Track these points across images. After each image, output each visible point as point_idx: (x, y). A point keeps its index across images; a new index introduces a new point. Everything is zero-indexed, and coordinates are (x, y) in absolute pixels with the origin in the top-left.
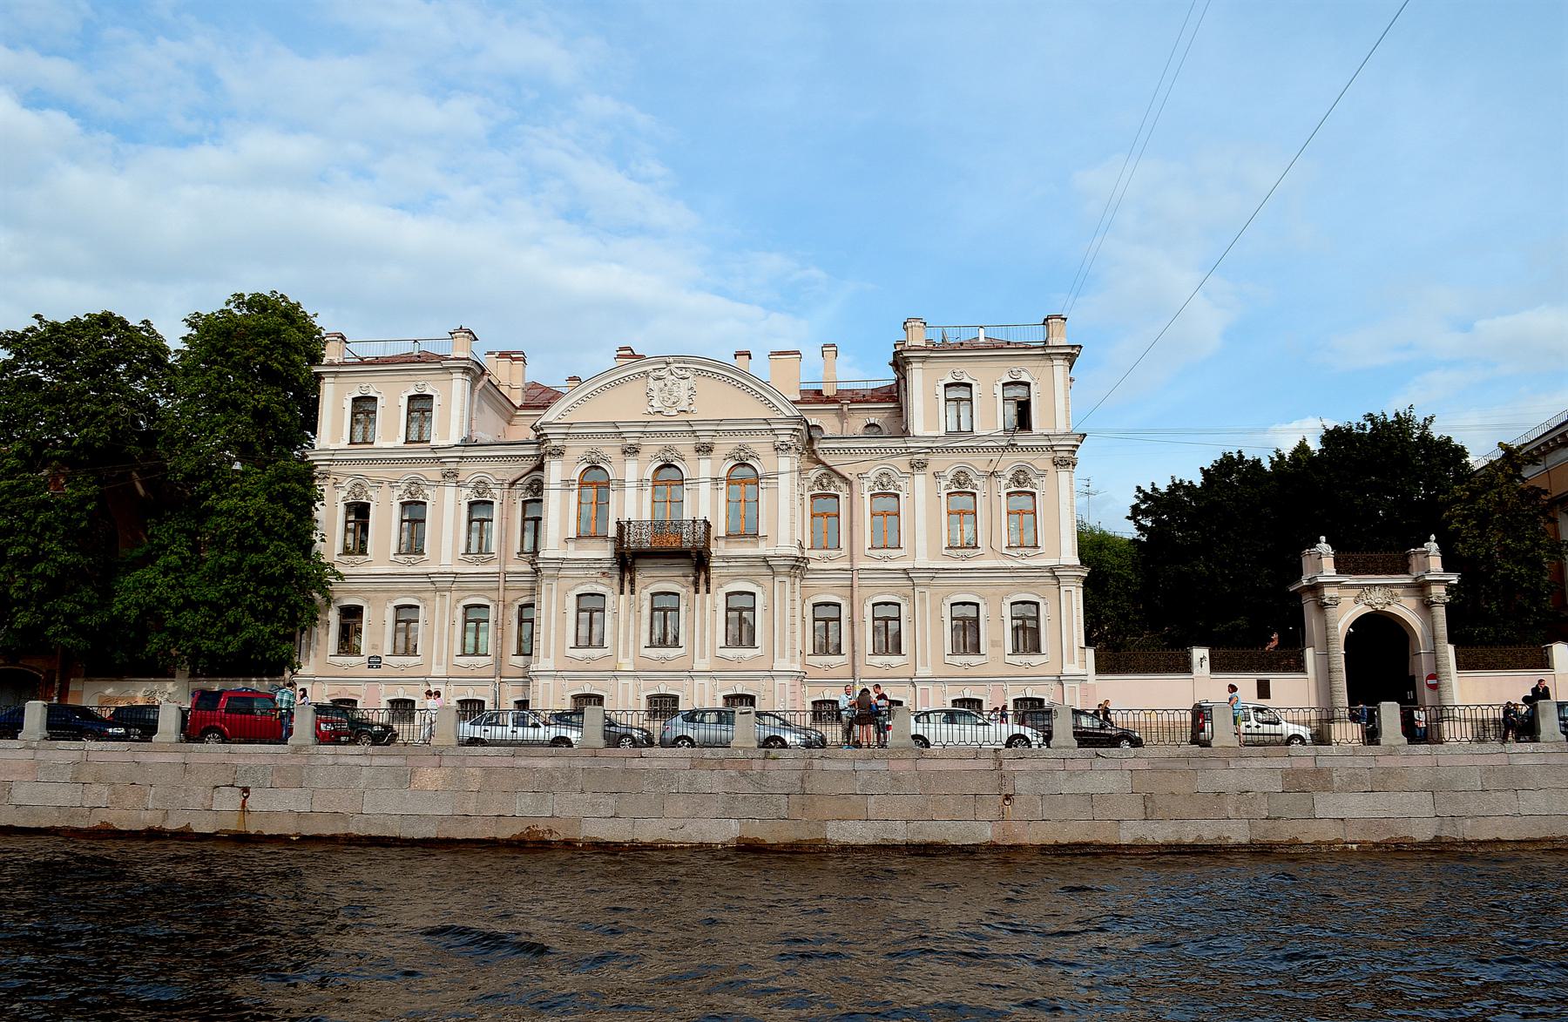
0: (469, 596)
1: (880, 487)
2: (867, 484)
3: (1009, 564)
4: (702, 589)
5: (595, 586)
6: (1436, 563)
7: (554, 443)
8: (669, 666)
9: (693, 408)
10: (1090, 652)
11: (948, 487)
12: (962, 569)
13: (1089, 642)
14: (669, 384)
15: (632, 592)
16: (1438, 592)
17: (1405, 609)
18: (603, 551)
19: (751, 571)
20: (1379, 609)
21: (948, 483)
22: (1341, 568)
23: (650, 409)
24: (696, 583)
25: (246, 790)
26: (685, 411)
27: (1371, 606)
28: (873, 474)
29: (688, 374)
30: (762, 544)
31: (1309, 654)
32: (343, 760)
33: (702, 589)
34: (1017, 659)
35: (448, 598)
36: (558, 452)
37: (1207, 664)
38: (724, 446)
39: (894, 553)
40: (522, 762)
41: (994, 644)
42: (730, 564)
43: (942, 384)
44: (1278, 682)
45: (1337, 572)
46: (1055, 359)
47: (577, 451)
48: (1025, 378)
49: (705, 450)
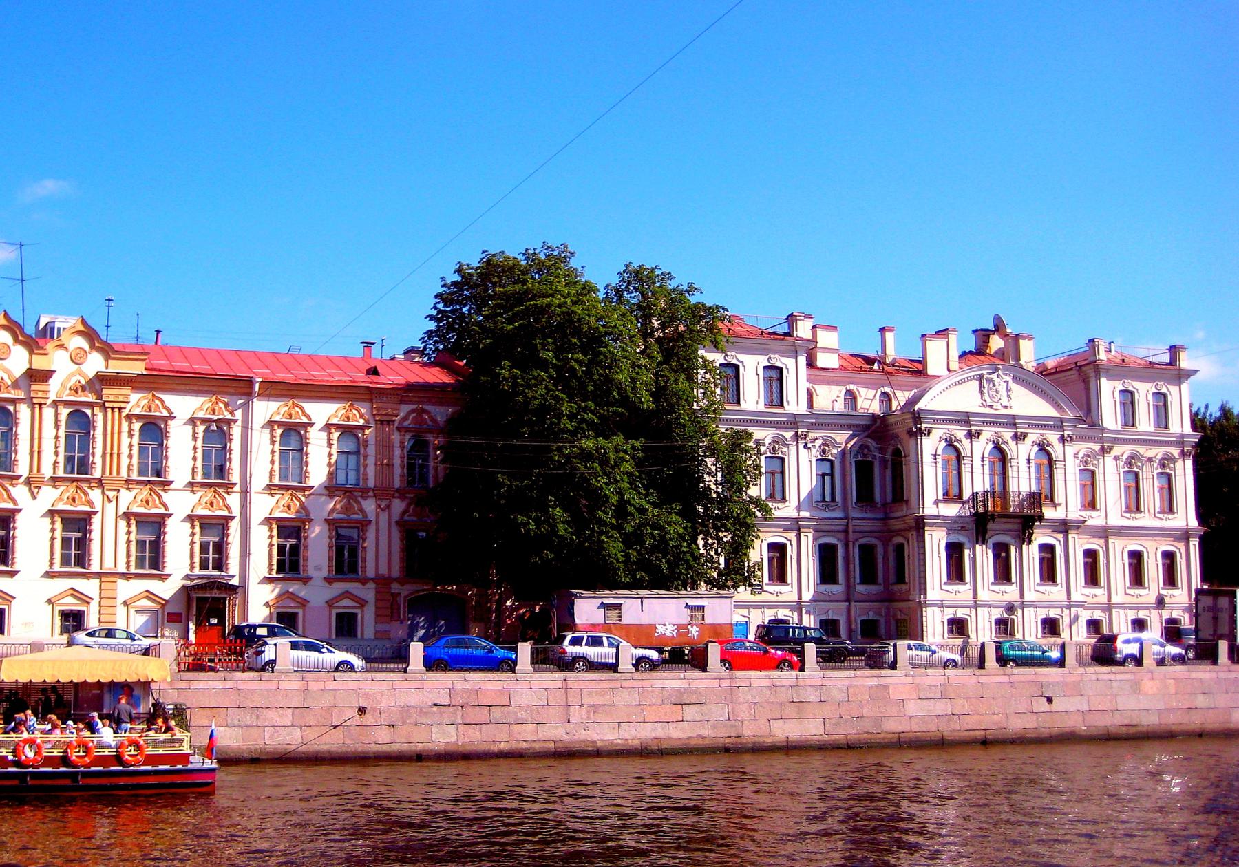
23: (984, 403)
25: (1050, 700)
32: (1100, 677)
38: (1033, 436)
40: (1194, 675)
47: (939, 432)
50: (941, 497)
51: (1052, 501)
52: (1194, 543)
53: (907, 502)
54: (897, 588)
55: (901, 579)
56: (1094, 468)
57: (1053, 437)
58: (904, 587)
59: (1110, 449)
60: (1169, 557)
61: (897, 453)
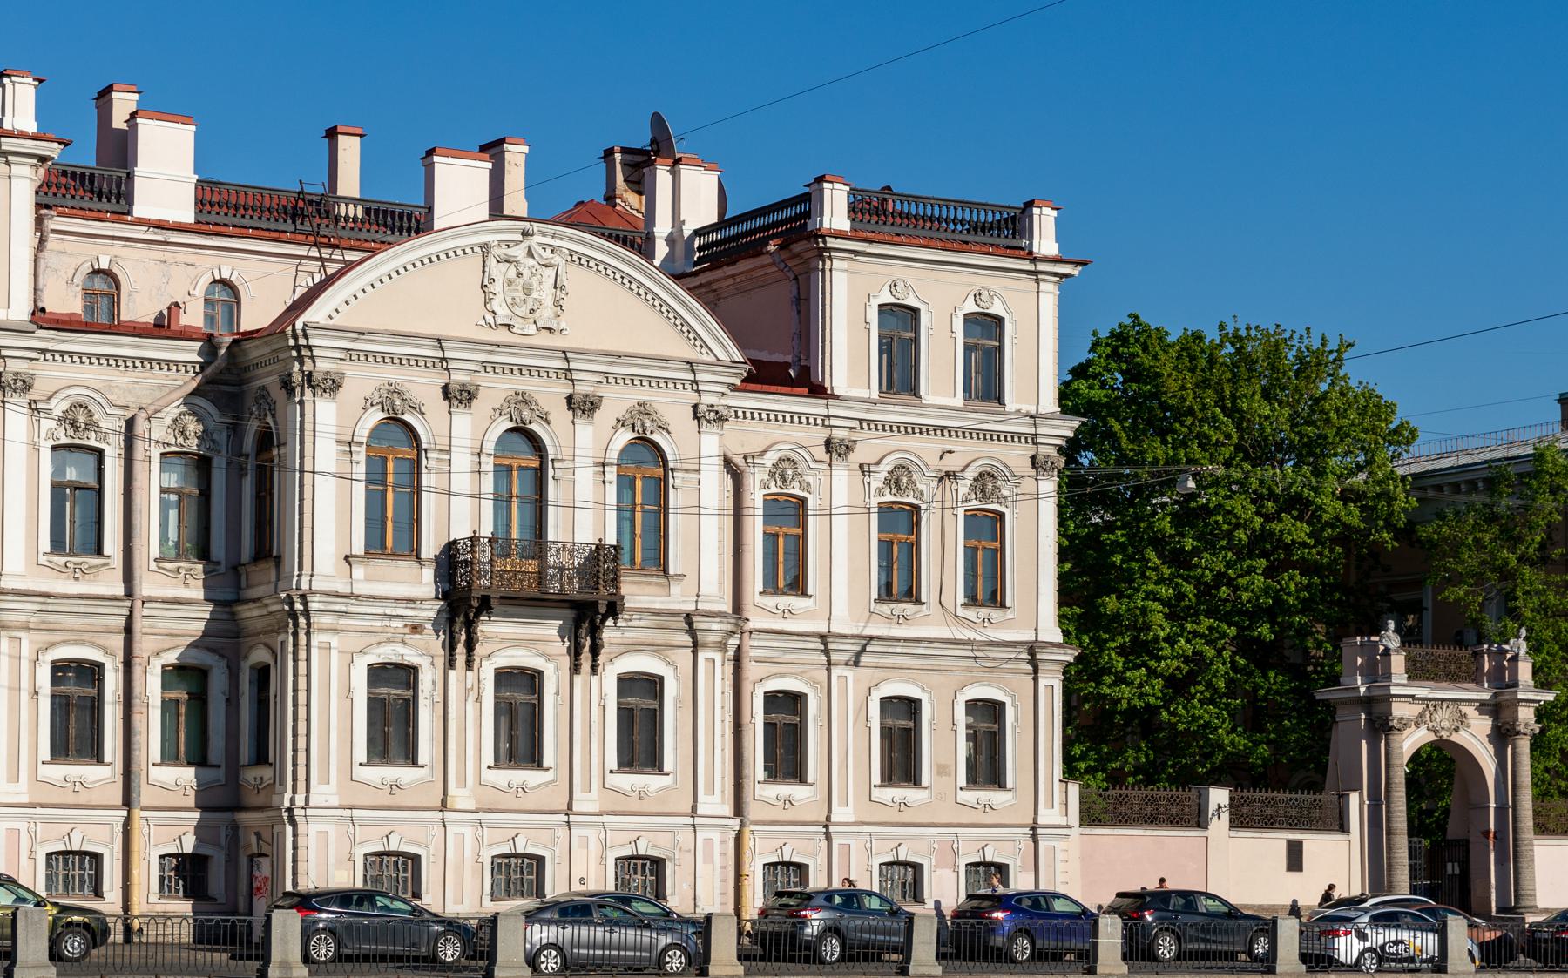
0: (65, 642)
1: (780, 483)
2: (761, 475)
3: (972, 636)
4: (586, 665)
5: (401, 649)
6: (1525, 671)
7: (322, 365)
8: (527, 802)
9: (563, 325)
10: (1074, 789)
11: (880, 492)
12: (906, 640)
13: (1070, 772)
14: (526, 273)
15: (469, 664)
16: (1526, 715)
17: (1475, 737)
18: (421, 583)
19: (660, 637)
20: (1445, 737)
21: (881, 484)
22: (1416, 672)
23: (490, 318)
24: (576, 652)
26: (550, 329)
27: (1436, 732)
28: (770, 459)
29: (557, 259)
30: (675, 589)
31: (1356, 803)
33: (586, 665)
34: (969, 796)
35: (25, 643)
36: (333, 385)
37: (1225, 816)
39: (797, 603)
41: (941, 770)
42: (630, 624)
43: (875, 303)
44: (1316, 845)
45: (1409, 678)
46: (1045, 281)
48: (997, 309)
49: (582, 406)
50: (359, 547)
51: (658, 563)
52: (1052, 683)
53: (278, 560)
54: (251, 775)
55: (261, 757)
56: (804, 494)
57: (673, 407)
58: (266, 773)
59: (848, 447)
60: (988, 713)
61: (266, 440)
